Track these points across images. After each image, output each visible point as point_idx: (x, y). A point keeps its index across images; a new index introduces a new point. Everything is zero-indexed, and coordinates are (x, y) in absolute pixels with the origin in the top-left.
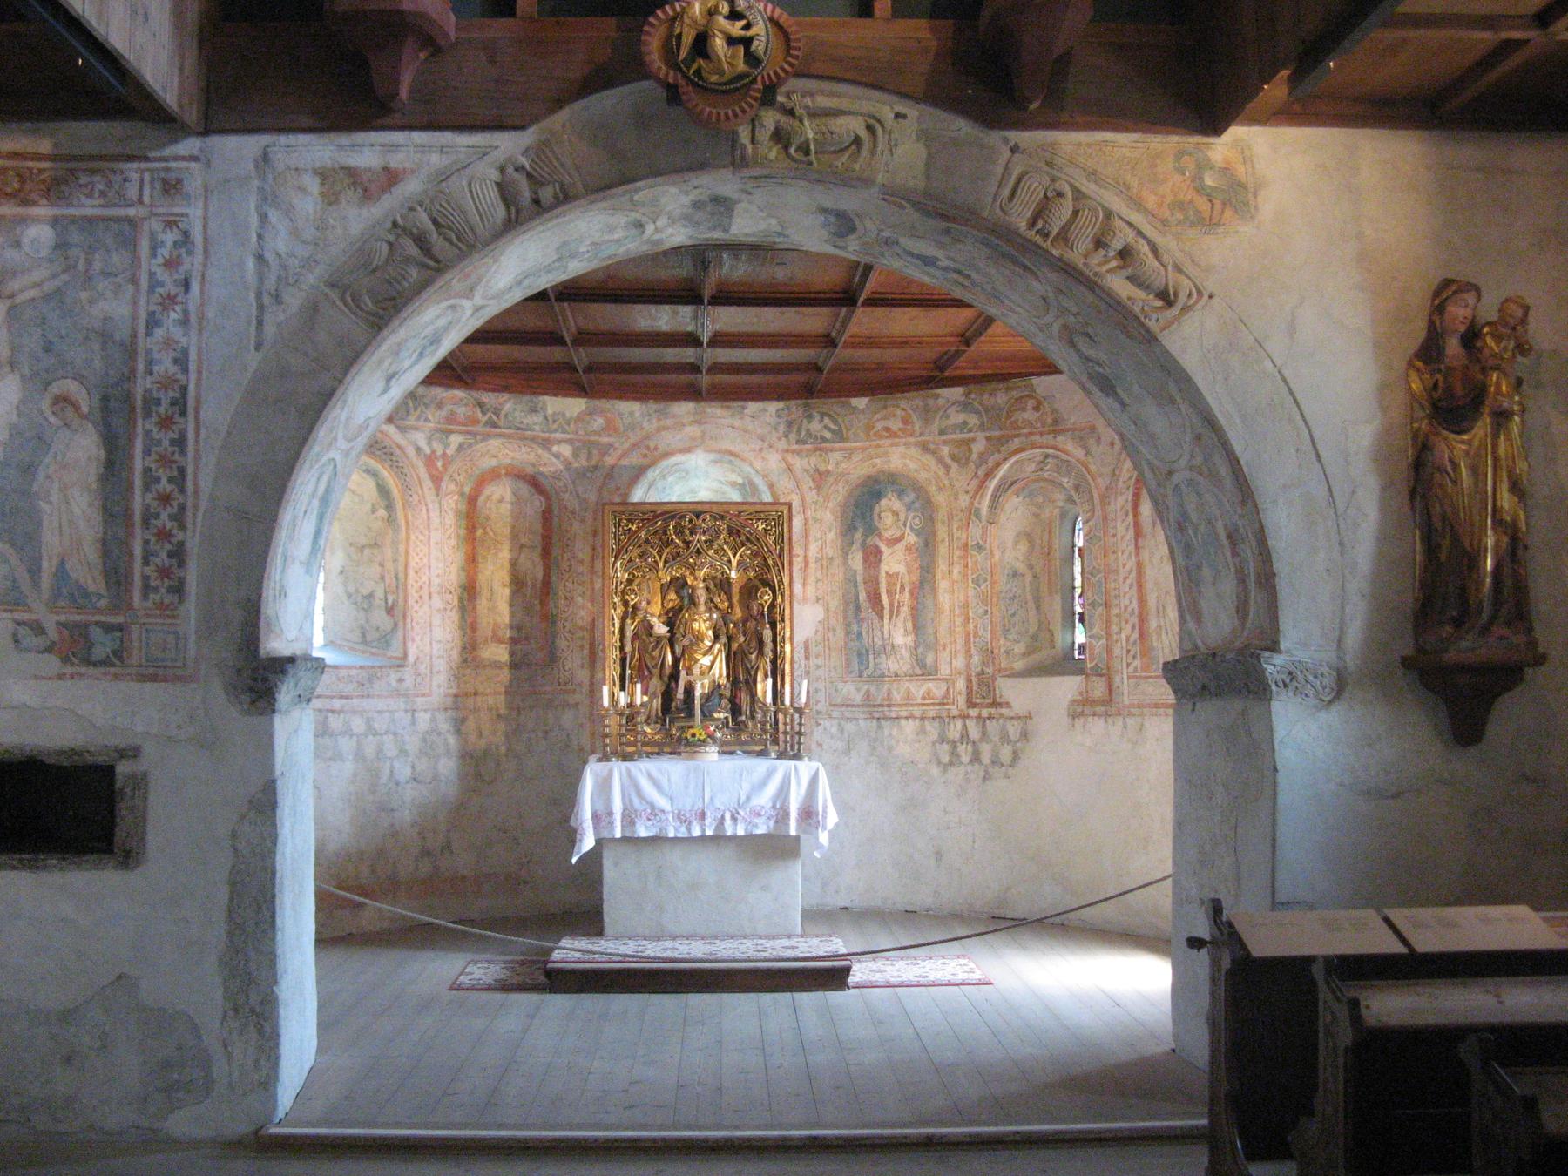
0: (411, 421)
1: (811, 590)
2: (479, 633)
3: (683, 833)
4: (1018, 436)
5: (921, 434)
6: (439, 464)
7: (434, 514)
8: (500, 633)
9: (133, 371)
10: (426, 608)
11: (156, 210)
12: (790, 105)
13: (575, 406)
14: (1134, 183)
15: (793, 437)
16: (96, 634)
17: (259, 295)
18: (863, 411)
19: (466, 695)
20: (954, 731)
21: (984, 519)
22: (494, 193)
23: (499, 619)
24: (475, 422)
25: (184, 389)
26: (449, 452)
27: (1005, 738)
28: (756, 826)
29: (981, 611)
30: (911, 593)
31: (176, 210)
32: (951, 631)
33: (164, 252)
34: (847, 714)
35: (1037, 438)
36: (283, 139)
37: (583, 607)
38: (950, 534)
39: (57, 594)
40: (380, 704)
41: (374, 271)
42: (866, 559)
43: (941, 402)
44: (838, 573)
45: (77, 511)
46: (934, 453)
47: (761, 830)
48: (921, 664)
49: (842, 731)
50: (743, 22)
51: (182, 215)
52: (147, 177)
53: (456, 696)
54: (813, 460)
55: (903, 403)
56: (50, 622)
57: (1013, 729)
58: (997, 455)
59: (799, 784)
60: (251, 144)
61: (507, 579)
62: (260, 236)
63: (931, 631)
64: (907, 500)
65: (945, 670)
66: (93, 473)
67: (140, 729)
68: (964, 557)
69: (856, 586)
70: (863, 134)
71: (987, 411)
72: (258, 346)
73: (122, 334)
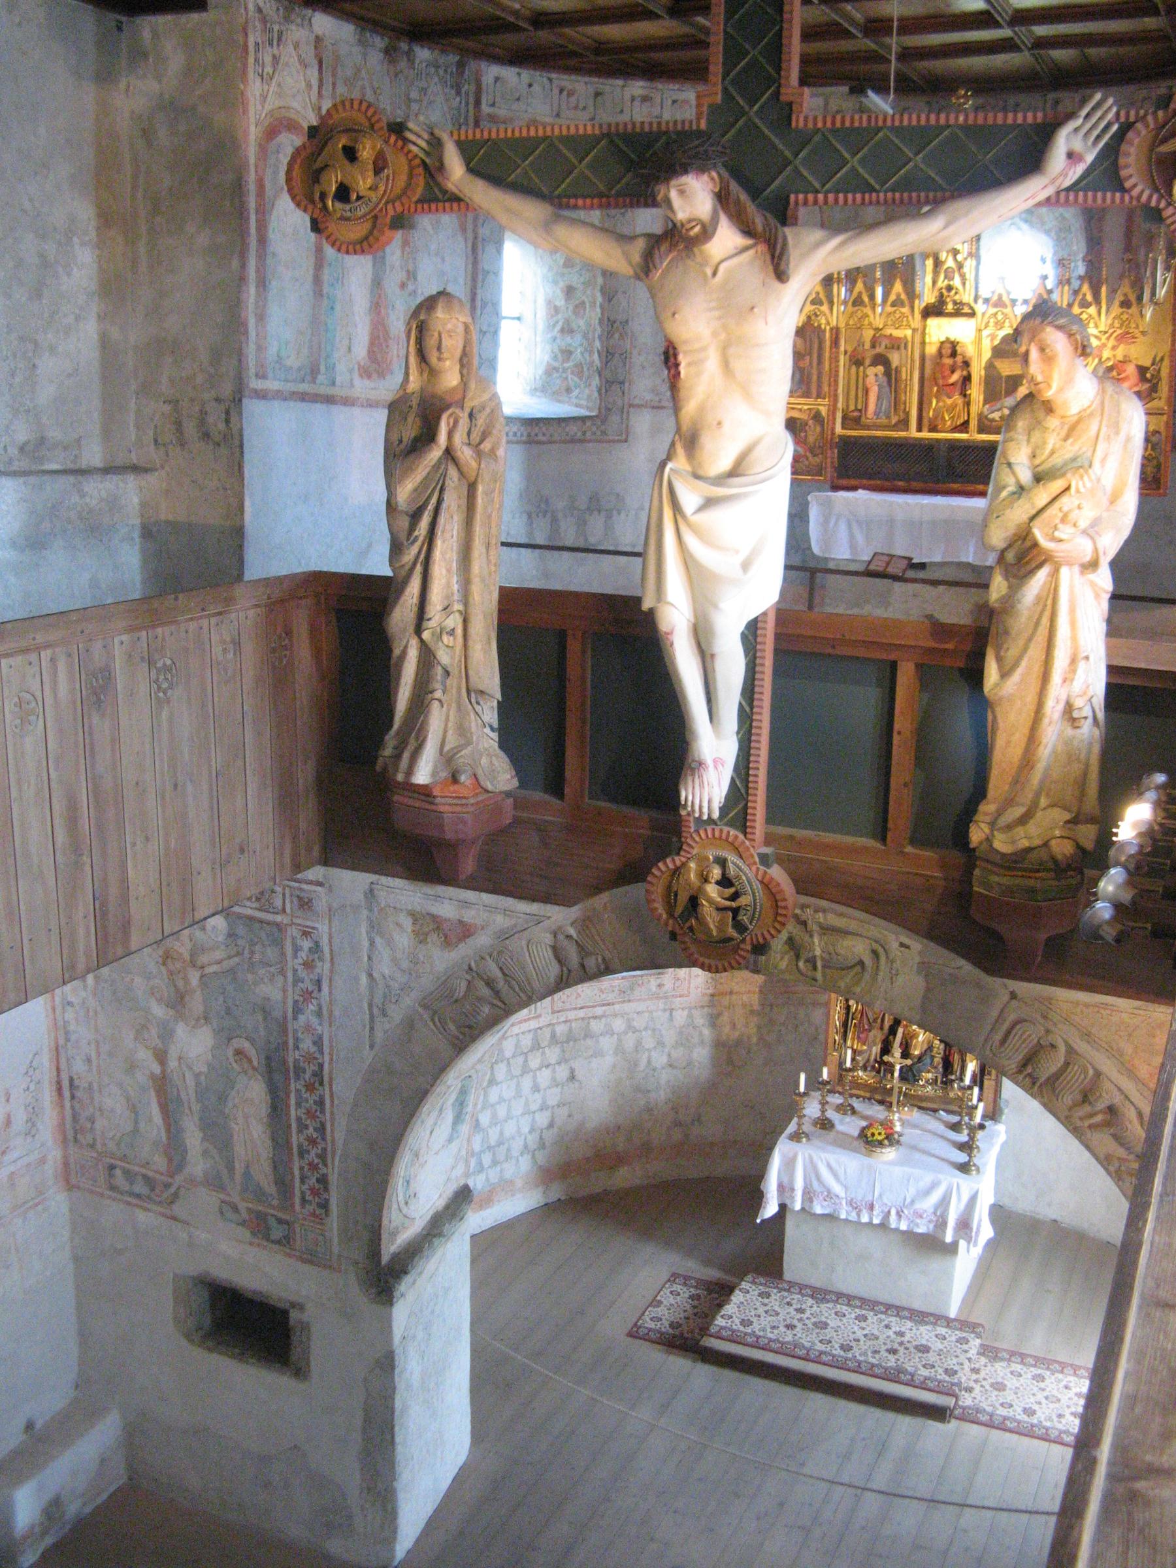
3: (853, 1216)
9: (286, 1043)
11: (295, 920)
12: (804, 918)
14: (1129, 1049)
16: (272, 1222)
17: (370, 1005)
19: (722, 994)
22: (549, 954)
25: (321, 1066)
28: (917, 1225)
31: (308, 923)
33: (303, 955)
36: (384, 880)
39: (245, 1189)
40: (641, 1006)
41: (456, 1001)
45: (256, 1136)
47: (921, 1230)
50: (732, 890)
51: (313, 928)
52: (287, 891)
53: (712, 995)
56: (242, 1206)
59: (959, 1199)
60: (363, 879)
62: (370, 958)
66: (264, 1110)
67: (304, 1293)
70: (868, 960)
72: (372, 1047)
73: (277, 1014)
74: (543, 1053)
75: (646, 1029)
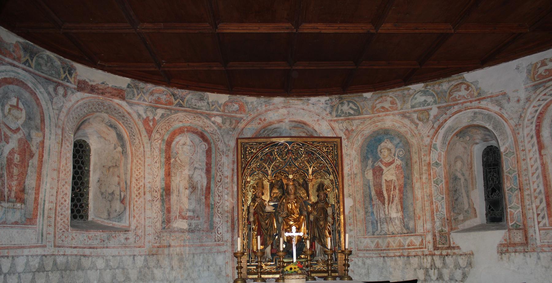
0: (135, 100)
2: (172, 214)
4: (457, 104)
5: (402, 109)
6: (151, 124)
7: (147, 149)
8: (183, 214)
10: (142, 199)
13: (223, 98)
15: (334, 114)
18: (370, 99)
21: (439, 149)
23: (183, 207)
24: (171, 103)
26: (157, 118)
29: (440, 198)
30: (400, 190)
32: (423, 209)
34: (367, 255)
35: (468, 104)
37: (227, 200)
38: (420, 158)
40: (115, 252)
42: (374, 174)
43: (411, 92)
46: (408, 118)
48: (406, 227)
49: (364, 263)
54: (345, 124)
55: (391, 94)
58: (444, 116)
61: (187, 186)
63: (411, 209)
64: (395, 142)
65: (420, 230)
68: (429, 170)
69: (369, 188)
71: (437, 94)
74: (47, 276)
75: (118, 268)
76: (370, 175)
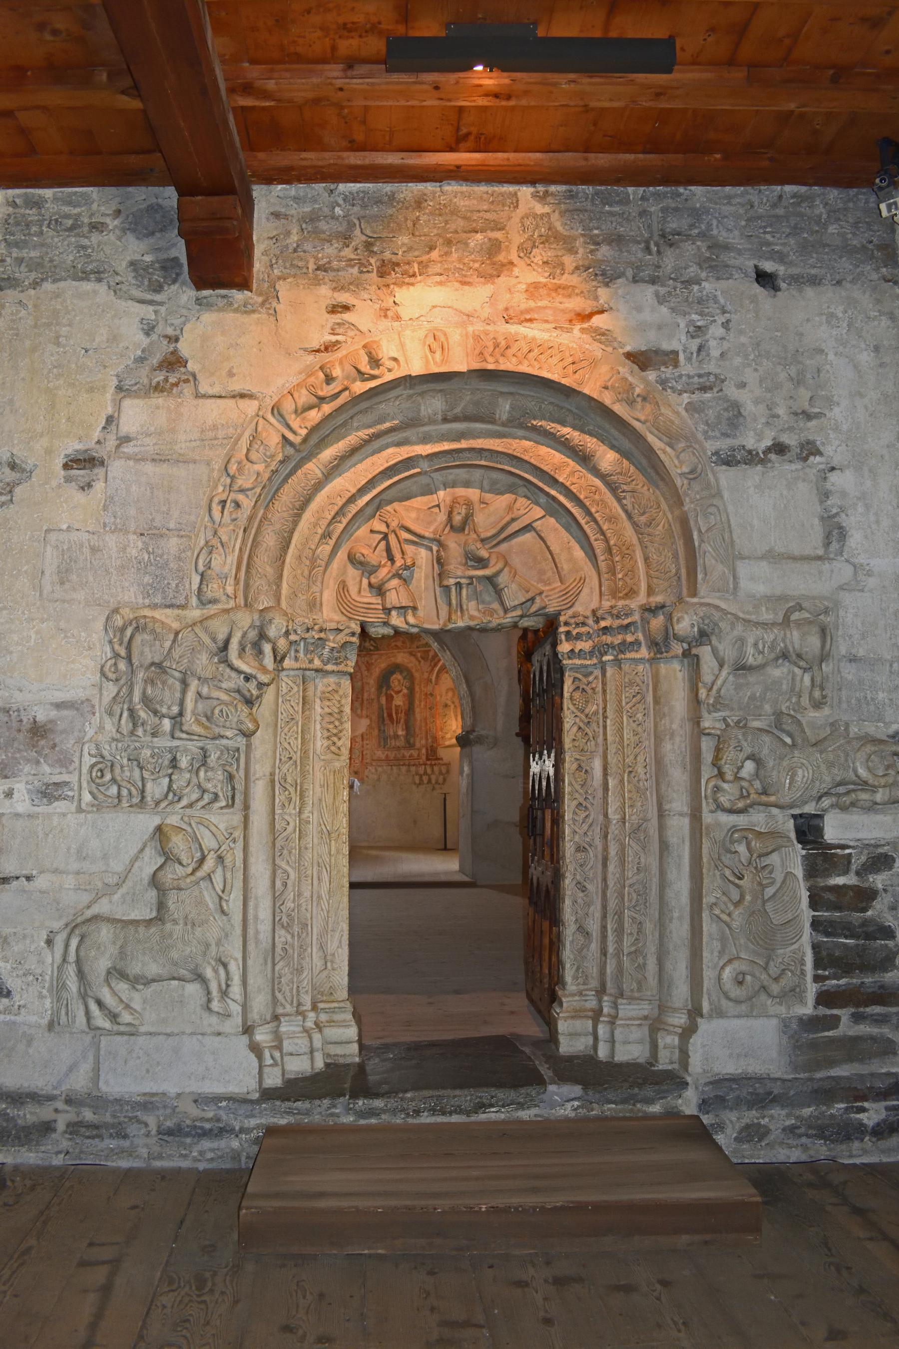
1: (364, 712)
20: (421, 770)
27: (441, 773)
44: (375, 705)
48: (408, 742)
57: (444, 769)
65: (418, 745)
76: (383, 700)
